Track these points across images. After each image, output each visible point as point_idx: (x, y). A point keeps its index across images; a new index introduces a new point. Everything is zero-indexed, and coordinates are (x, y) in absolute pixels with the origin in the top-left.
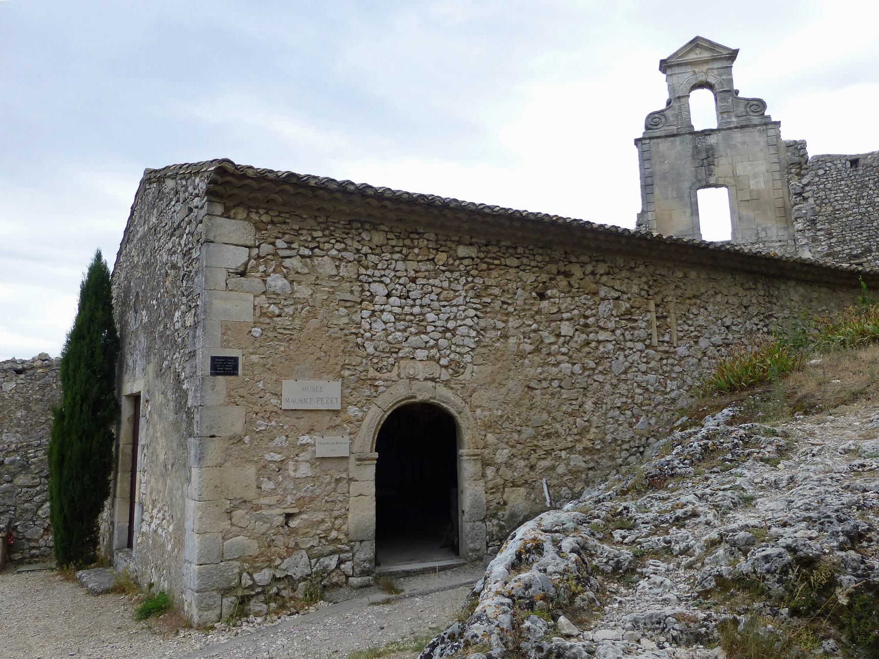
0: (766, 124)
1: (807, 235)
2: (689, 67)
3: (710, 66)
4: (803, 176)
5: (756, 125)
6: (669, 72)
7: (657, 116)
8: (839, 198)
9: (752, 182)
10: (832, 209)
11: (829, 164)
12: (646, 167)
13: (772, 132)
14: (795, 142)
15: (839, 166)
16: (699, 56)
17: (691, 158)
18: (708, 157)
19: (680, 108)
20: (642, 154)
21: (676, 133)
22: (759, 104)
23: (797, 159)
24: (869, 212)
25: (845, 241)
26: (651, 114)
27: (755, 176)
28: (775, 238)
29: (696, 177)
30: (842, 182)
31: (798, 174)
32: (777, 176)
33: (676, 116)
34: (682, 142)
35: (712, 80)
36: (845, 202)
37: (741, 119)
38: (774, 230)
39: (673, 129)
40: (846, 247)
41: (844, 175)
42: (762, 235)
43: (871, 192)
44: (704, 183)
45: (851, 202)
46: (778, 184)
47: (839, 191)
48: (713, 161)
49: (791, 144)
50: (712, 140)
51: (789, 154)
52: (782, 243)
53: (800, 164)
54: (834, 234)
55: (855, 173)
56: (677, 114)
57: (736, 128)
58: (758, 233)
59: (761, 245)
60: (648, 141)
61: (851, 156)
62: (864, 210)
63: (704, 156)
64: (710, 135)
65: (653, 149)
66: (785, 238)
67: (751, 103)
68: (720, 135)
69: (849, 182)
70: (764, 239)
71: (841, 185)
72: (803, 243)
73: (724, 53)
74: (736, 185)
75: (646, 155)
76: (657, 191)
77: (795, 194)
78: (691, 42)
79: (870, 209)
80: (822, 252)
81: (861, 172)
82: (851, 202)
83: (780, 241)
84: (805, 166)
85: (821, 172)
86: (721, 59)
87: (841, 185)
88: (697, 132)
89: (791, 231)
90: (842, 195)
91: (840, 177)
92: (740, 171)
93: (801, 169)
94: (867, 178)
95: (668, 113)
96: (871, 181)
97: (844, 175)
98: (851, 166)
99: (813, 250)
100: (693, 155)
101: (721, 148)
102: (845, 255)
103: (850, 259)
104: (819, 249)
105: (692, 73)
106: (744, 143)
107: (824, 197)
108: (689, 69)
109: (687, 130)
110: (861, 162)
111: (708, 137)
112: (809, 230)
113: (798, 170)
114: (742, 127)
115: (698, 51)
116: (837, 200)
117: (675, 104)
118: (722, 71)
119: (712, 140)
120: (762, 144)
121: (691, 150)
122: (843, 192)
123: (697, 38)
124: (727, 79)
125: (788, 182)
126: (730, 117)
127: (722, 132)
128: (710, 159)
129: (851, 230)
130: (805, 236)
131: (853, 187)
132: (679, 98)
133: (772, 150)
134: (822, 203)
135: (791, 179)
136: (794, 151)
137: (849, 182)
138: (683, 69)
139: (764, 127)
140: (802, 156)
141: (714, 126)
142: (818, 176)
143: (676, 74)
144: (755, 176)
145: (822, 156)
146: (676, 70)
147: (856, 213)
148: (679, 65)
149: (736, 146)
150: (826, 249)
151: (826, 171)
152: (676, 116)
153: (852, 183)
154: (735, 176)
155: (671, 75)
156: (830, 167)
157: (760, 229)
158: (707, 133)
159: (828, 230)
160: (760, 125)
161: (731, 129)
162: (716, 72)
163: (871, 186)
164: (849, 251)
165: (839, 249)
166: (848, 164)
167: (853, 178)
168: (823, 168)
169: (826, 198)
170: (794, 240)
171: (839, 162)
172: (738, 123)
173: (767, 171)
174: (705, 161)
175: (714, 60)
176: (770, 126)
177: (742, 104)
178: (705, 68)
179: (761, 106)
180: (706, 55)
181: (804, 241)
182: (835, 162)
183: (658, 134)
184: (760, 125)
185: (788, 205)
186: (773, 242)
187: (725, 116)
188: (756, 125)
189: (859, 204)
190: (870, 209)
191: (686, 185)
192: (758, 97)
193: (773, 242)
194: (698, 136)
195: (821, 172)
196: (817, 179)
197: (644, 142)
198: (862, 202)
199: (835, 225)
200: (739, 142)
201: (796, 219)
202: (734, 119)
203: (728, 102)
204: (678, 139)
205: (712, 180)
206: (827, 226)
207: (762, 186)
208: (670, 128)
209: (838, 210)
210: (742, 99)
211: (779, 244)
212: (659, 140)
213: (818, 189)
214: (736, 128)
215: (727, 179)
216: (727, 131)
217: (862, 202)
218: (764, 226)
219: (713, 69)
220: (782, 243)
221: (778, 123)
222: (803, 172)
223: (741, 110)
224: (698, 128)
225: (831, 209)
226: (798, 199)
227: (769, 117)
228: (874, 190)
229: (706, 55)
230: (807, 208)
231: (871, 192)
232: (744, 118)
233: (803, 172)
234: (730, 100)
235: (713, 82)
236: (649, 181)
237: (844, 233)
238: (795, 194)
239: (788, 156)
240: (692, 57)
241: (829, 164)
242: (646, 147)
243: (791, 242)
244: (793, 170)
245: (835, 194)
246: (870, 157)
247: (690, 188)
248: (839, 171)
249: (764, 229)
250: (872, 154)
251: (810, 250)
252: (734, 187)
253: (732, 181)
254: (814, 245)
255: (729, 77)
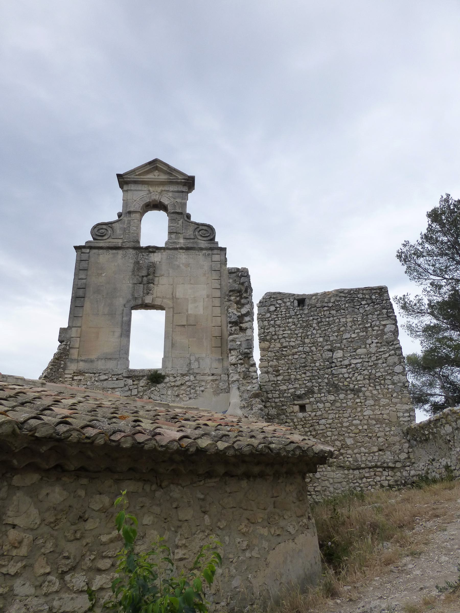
0: (211, 249)
1: (239, 370)
2: (146, 186)
3: (166, 188)
4: (243, 305)
5: (201, 249)
6: (125, 188)
7: (104, 227)
8: (286, 335)
9: (191, 306)
10: (280, 346)
11: (279, 302)
12: (80, 277)
13: (216, 258)
14: (238, 269)
15: (288, 304)
16: (156, 177)
17: (130, 274)
18: (148, 275)
19: (129, 223)
20: (79, 261)
21: (120, 245)
22: (208, 229)
23: (236, 286)
24: (312, 351)
25: (290, 379)
26: (98, 225)
27: (195, 300)
28: (207, 371)
29: (133, 295)
30: (290, 320)
31: (238, 303)
32: (217, 302)
33: (124, 230)
34: (124, 256)
35: (165, 201)
36: (292, 340)
37: (188, 241)
38: (208, 361)
39: (119, 242)
40: (291, 386)
41: (292, 313)
42: (195, 365)
43: (314, 332)
44: (140, 302)
45: (296, 340)
46: (217, 311)
47: (287, 328)
48: (153, 280)
49: (233, 271)
50: (156, 258)
51: (231, 281)
52: (215, 377)
53: (239, 291)
54: (281, 371)
55: (301, 312)
56: (125, 228)
57: (181, 248)
58: (190, 363)
59: (192, 378)
60: (88, 251)
61: (298, 295)
62: (308, 349)
63: (144, 273)
64: (154, 252)
65: (92, 260)
66: (219, 371)
67: (201, 227)
68: (165, 254)
69: (296, 320)
70: (196, 371)
71: (289, 323)
72: (234, 379)
73: (180, 177)
74: (173, 308)
75: (84, 265)
76: (87, 305)
77: (230, 323)
78: (150, 163)
79: (314, 348)
80: (251, 391)
81: (306, 312)
82: (296, 340)
83: (213, 375)
84: (245, 295)
85: (272, 308)
86: (177, 183)
87: (289, 323)
88: (142, 248)
89: (226, 364)
90: (289, 332)
91: (288, 315)
92: (179, 293)
93: (241, 298)
94: (311, 318)
95: (116, 226)
96: (315, 321)
97: (292, 313)
98: (299, 305)
99: (242, 388)
100: (133, 271)
101: (163, 269)
102: (289, 395)
103: (294, 400)
104: (249, 388)
105: (147, 192)
106: (187, 265)
107: (273, 333)
108: (145, 188)
109: (131, 245)
110: (307, 302)
111: (152, 255)
112: (241, 364)
113: (238, 299)
114: (188, 249)
115: (156, 173)
116: (284, 337)
117: (125, 219)
118: (177, 194)
119: (156, 258)
120: (206, 268)
121: (132, 265)
122: (290, 330)
123: (155, 161)
124: (181, 203)
125: (227, 310)
126: (178, 238)
127: (167, 251)
128: (150, 277)
129: (296, 369)
130: (237, 371)
131: (299, 325)
132: (130, 213)
133: (215, 275)
134: (271, 339)
135: (229, 307)
136: (235, 278)
137: (296, 320)
138: (140, 187)
139: (210, 252)
140: (243, 284)
141: (162, 244)
142: (269, 312)
143: (131, 190)
144: (195, 300)
145: (274, 293)
146: (132, 187)
147: (301, 351)
148: (135, 182)
149: (178, 266)
150: (256, 388)
151: (276, 308)
152: (124, 230)
153: (298, 321)
154: (173, 298)
155: (127, 191)
156: (280, 304)
157: (193, 358)
158: (151, 250)
159: (275, 366)
160: (206, 249)
161: (176, 249)
162: (170, 194)
163: (314, 325)
164: (293, 390)
165: (284, 387)
166: (296, 303)
167: (299, 316)
168: (274, 305)
169: (275, 334)
170: (228, 375)
171: (288, 300)
172: (184, 245)
173: (208, 296)
174: (145, 279)
175: (171, 183)
176: (215, 252)
177: (192, 228)
178: (159, 189)
179: (210, 231)
180: (163, 177)
181: (236, 377)
182: (285, 300)
183: (101, 245)
184: (206, 249)
185: (226, 333)
186: (204, 375)
187: (173, 236)
188: (201, 249)
189: (304, 343)
190: (314, 348)
191: (120, 302)
192: (208, 223)
193: (204, 375)
194: (142, 252)
195: (272, 308)
196: (268, 315)
197: (84, 250)
198: (307, 341)
199: (282, 362)
200: (183, 264)
201: (230, 350)
202: (182, 241)
203: (178, 224)
204: (120, 252)
205: (148, 300)
206: (275, 363)
207: (201, 311)
208: (116, 240)
209: (285, 347)
210: (192, 223)
211: (211, 378)
212: (101, 251)
213: (269, 325)
214: (181, 248)
215: (165, 300)
216: (172, 251)
217: (307, 341)
218: (197, 356)
219: (168, 191)
220: (215, 377)
221: (224, 250)
222: (243, 301)
223: (190, 232)
224: (144, 243)
225: (279, 345)
226: (233, 329)
227: (217, 243)
228: (317, 330)
229: (163, 177)
230: (242, 339)
231: (314, 332)
232: (192, 241)
233: (243, 301)
234: (180, 222)
235: (166, 203)
236: (81, 293)
237: (290, 371)
238: (230, 323)
239: (229, 283)
240: (150, 177)
241: (279, 302)
242: (84, 257)
243: (224, 377)
244: (232, 298)
245: (283, 331)
246: (314, 297)
247: (124, 305)
248: (288, 309)
249: (197, 360)
250: (316, 295)
251: (239, 388)
252: (172, 309)
253: (170, 303)
254: (244, 382)
255: (183, 201)
